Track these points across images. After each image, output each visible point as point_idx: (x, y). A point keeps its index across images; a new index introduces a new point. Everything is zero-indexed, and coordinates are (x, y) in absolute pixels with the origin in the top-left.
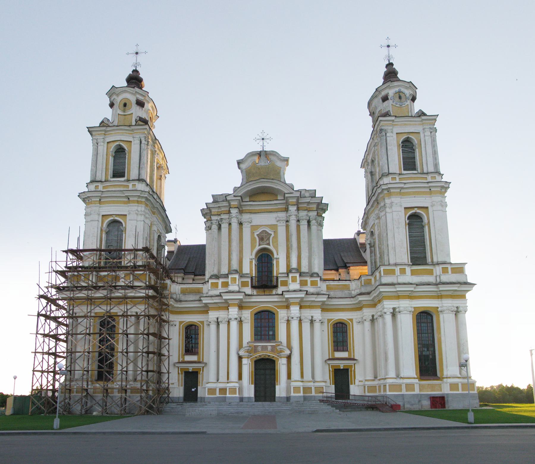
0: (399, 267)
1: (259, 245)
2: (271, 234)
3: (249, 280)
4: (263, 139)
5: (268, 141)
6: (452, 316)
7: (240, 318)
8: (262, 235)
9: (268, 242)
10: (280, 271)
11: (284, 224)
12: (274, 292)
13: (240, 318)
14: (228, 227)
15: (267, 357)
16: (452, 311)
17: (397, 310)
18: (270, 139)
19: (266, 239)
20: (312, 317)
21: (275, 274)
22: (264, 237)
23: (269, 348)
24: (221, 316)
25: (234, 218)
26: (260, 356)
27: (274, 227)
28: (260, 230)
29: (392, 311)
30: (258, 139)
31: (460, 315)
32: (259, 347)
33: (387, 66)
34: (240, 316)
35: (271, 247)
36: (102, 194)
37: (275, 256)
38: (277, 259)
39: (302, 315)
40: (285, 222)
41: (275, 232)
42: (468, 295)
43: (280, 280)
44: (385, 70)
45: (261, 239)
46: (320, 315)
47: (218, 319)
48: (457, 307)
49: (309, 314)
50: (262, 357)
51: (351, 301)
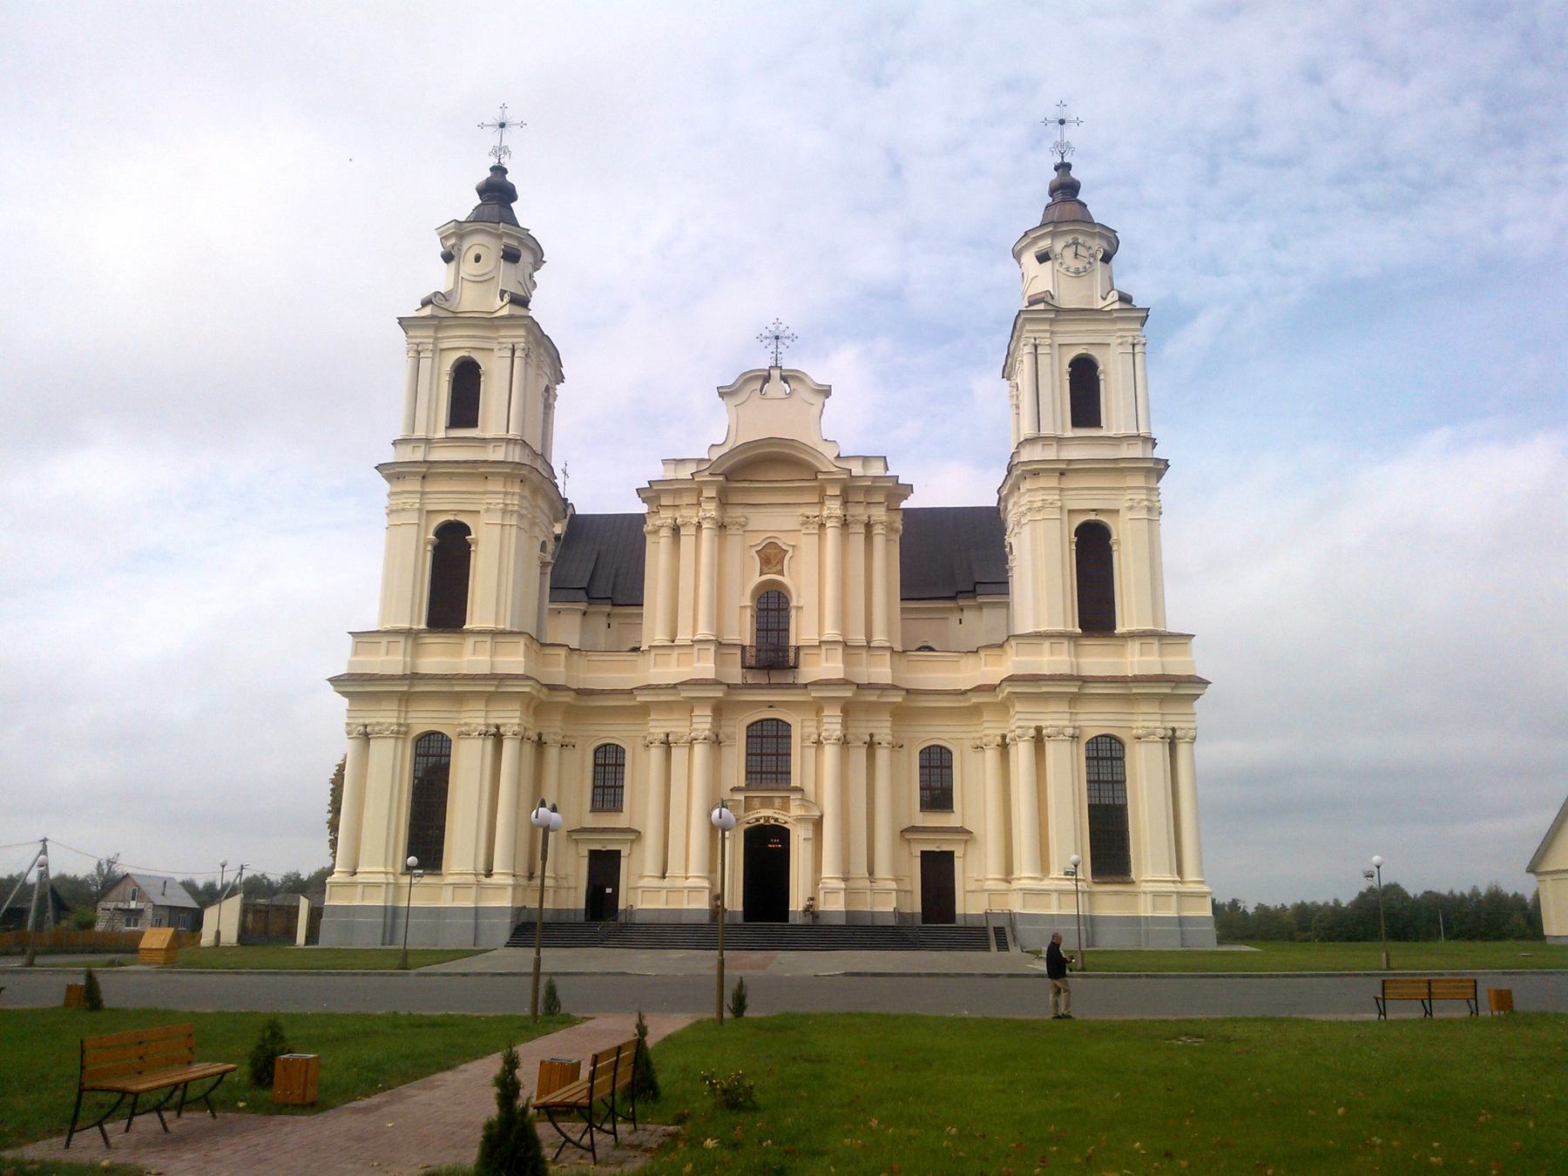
2: (787, 551)
4: (777, 338)
5: (787, 342)
7: (717, 736)
8: (768, 551)
9: (780, 568)
13: (717, 736)
14: (694, 533)
15: (772, 822)
16: (1162, 738)
19: (775, 562)
20: (872, 736)
21: (793, 642)
26: (758, 820)
30: (766, 338)
32: (755, 799)
34: (716, 731)
35: (783, 579)
36: (428, 468)
37: (793, 603)
38: (799, 608)
39: (851, 730)
40: (817, 526)
46: (888, 731)
47: (668, 735)
48: (1174, 730)
49: (864, 730)
50: (762, 821)
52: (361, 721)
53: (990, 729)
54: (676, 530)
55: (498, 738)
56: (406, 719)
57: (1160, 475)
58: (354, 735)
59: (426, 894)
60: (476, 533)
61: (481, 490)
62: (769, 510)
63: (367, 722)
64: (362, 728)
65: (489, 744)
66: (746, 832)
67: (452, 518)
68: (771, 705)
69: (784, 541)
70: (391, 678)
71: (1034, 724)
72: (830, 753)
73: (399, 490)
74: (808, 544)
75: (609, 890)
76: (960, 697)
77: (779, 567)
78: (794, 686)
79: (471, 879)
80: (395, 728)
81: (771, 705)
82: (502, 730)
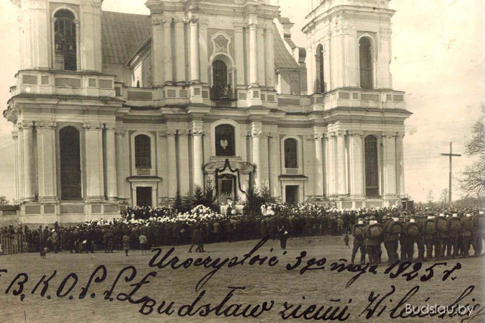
0: (352, 92)
3: (208, 90)
6: (392, 140)
10: (238, 83)
11: (242, 30)
24: (180, 128)
27: (230, 32)
28: (217, 35)
31: (398, 139)
35: (228, 55)
41: (233, 39)
42: (406, 122)
43: (239, 91)
55: (104, 131)
56: (55, 119)
57: (391, 15)
64: (32, 124)
65: (101, 133)
74: (239, 36)
78: (236, 108)
80: (52, 124)
81: (227, 117)
82: (106, 126)
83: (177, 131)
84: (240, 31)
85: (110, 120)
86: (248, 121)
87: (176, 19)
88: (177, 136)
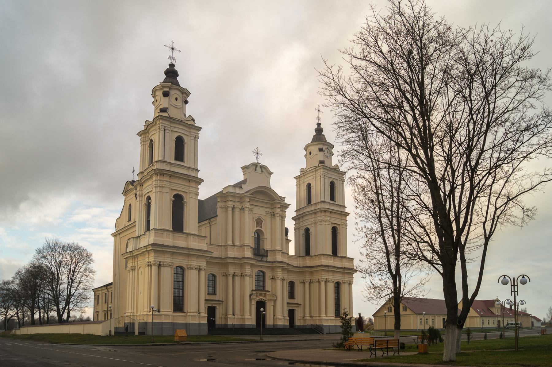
1: (257, 227)
5: (260, 155)
12: (265, 259)
17: (328, 280)
18: (261, 155)
22: (259, 222)
23: (263, 294)
24: (237, 271)
25: (247, 208)
26: (259, 299)
29: (325, 280)
31: (350, 285)
33: (170, 65)
38: (266, 239)
44: (168, 67)
45: (257, 223)
48: (350, 281)
50: (260, 300)
51: (299, 270)
52: (159, 260)
53: (308, 278)
54: (233, 208)
58: (156, 265)
59: (179, 318)
60: (186, 200)
61: (188, 185)
62: (257, 207)
63: (161, 260)
66: (256, 302)
67: (179, 193)
68: (261, 267)
69: (263, 218)
70: (183, 248)
71: (326, 278)
72: (279, 282)
73: (162, 179)
75: (212, 319)
76: (300, 269)
77: (261, 226)
78: (266, 262)
79: (196, 314)
83: (234, 273)
84: (269, 216)
85: (203, 263)
86: (273, 269)
87: (236, 206)
88: (234, 276)
